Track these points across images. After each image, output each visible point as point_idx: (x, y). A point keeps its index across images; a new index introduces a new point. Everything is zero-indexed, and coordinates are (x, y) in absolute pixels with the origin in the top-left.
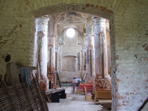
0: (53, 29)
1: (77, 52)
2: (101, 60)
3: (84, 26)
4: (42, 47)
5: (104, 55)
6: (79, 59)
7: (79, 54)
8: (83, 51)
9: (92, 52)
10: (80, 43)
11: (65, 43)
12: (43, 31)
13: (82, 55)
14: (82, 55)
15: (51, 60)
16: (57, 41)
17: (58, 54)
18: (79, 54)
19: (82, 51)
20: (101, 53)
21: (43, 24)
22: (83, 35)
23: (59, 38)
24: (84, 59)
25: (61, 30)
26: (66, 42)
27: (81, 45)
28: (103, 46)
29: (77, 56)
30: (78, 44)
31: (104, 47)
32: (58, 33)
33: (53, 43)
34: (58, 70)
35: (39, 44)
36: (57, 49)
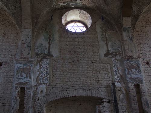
1: (105, 83)
7: (112, 89)
8: (129, 76)
10: (111, 50)
11: (58, 54)
13: (127, 91)
14: (127, 91)
17: (30, 93)
18: (112, 89)
19: (123, 79)
22: (120, 26)
24: (137, 106)
26: (60, 51)
27: (118, 58)
29: (106, 99)
30: (106, 55)
36: (29, 75)
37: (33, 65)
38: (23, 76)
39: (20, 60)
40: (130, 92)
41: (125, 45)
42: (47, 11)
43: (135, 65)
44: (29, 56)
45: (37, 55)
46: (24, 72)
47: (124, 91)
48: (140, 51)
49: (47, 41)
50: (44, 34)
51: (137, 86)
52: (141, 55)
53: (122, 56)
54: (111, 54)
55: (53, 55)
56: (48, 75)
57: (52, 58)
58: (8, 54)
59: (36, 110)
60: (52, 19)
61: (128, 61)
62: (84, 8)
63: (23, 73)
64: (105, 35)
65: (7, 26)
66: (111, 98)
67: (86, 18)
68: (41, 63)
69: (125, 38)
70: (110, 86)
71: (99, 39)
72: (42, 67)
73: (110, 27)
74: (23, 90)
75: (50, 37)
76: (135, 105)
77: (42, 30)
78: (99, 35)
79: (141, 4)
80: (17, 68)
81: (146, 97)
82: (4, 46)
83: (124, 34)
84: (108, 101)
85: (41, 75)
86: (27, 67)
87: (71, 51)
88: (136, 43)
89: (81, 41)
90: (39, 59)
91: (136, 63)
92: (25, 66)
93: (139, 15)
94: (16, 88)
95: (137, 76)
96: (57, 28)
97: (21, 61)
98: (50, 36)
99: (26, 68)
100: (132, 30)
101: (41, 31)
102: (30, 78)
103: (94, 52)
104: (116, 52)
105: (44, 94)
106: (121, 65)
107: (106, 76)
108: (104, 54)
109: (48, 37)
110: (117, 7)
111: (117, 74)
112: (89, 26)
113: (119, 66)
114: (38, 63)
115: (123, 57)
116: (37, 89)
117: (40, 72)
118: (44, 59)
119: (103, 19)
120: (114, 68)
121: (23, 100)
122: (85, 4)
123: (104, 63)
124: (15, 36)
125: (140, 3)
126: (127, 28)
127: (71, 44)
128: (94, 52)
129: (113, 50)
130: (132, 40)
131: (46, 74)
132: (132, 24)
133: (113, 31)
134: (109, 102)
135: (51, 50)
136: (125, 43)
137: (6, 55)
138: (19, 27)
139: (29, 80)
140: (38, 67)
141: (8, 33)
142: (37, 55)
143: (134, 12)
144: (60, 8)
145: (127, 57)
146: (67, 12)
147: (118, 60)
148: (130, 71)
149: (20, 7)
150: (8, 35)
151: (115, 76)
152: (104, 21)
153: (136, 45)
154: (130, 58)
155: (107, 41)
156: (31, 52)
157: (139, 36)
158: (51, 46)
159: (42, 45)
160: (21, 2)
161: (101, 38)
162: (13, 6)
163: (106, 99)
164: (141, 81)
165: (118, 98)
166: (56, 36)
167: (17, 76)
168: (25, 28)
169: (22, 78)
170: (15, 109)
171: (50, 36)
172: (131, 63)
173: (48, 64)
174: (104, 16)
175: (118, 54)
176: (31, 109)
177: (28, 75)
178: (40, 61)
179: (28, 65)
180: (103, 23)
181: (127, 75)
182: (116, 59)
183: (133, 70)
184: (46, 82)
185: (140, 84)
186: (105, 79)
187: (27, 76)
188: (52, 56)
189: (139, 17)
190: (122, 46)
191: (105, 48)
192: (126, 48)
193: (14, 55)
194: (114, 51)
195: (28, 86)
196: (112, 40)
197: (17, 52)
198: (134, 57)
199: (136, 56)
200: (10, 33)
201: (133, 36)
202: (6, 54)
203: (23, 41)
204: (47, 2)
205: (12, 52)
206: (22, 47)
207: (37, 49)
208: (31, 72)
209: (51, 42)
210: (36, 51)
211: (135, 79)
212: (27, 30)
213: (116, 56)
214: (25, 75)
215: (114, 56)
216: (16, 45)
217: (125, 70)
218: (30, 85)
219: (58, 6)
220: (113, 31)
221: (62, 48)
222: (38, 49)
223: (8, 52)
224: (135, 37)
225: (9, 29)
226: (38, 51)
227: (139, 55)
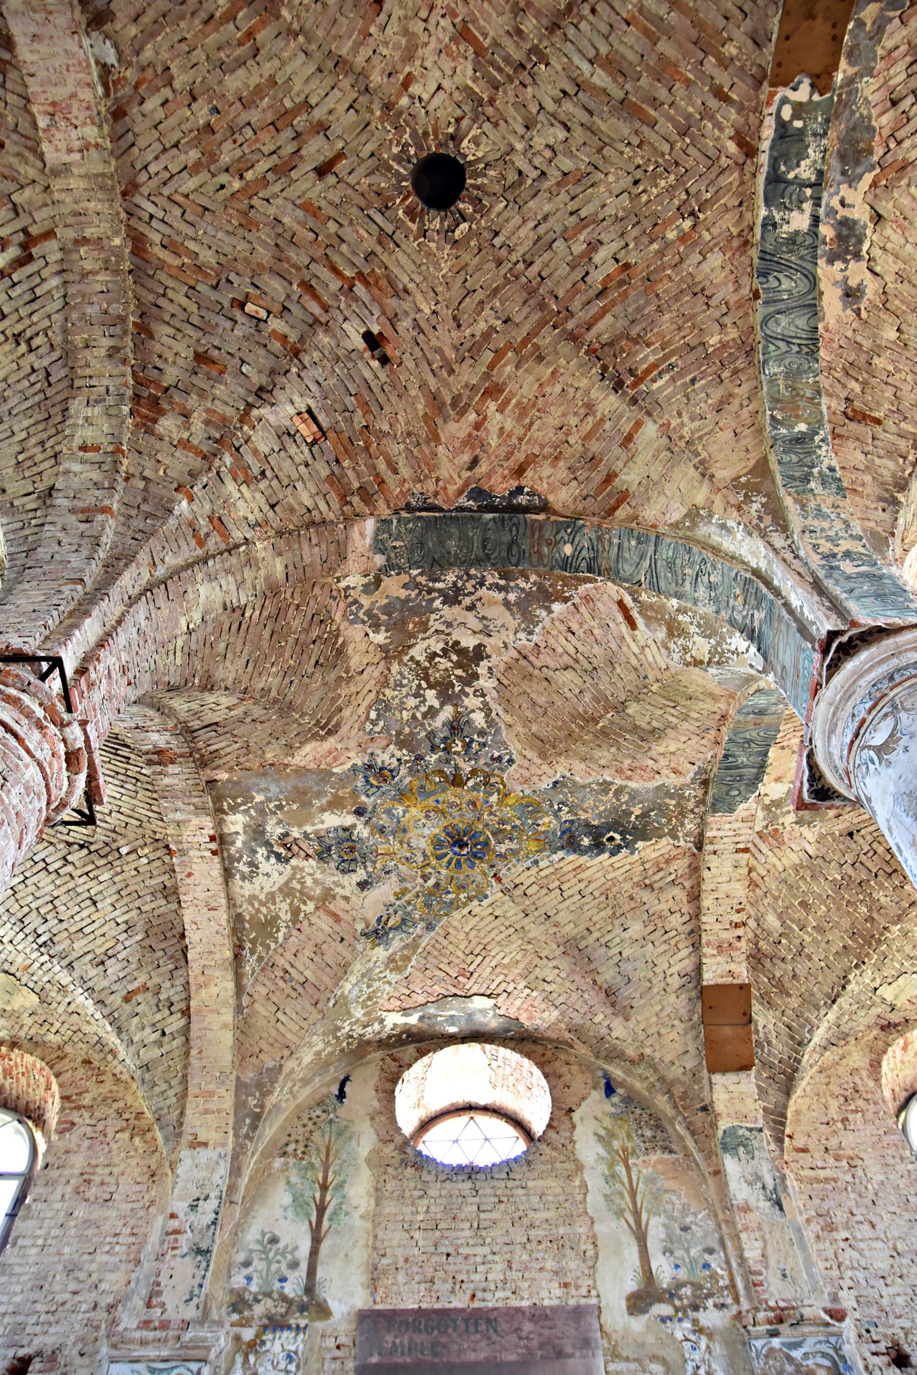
3: (695, 937)
16: (202, 1252)
27: (711, 1317)
32: (239, 1105)
39: (138, 1335)
41: (743, 1236)
42: (318, 1054)
44: (190, 1312)
48: (835, 1273)
49: (308, 1215)
50: (294, 1179)
52: (847, 1301)
53: (734, 1309)
54: (670, 1295)
57: (320, 1325)
58: (78, 1298)
60: (341, 1095)
61: (776, 1342)
62: (511, 1039)
64: (626, 1180)
65: (110, 1135)
67: (521, 1088)
68: (252, 1358)
69: (739, 1191)
71: (595, 1200)
73: (648, 1133)
75: (323, 1197)
77: (284, 1154)
78: (594, 1179)
79: (794, 1002)
82: (67, 1250)
87: (432, 1281)
88: (808, 1221)
89: (495, 1215)
90: (248, 1334)
91: (824, 1355)
93: (799, 1062)
97: (143, 1343)
98: (324, 1188)
100: (773, 1146)
101: (278, 1163)
103: (566, 1285)
104: (692, 1284)
109: (308, 1193)
110: (676, 1022)
112: (538, 1127)
114: (239, 1359)
115: (739, 1316)
118: (274, 1331)
119: (609, 1090)
122: (512, 1013)
123: (627, 1359)
124: (138, 1188)
125: (789, 995)
126: (740, 1132)
127: (438, 1234)
128: (566, 1285)
129: (677, 1266)
130: (779, 1204)
132: (765, 1109)
133: (671, 1152)
135: (319, 1274)
136: (741, 1220)
137: (63, 1304)
138: (167, 1139)
141: (107, 1171)
142: (239, 1303)
143: (769, 1043)
144: (389, 1037)
145: (761, 1315)
146: (426, 1060)
147: (710, 1336)
149: (186, 1030)
150: (102, 1184)
152: (615, 1099)
153: (809, 1234)
154: (781, 1321)
155: (637, 1214)
156: (206, 1283)
157: (818, 1181)
158: (325, 1247)
159: (274, 1240)
160: (188, 1008)
162: (148, 1030)
168: (197, 1144)
171: (324, 1188)
172: (797, 1354)
174: (617, 1072)
175: (710, 1295)
180: (613, 1110)
182: (699, 1330)
188: (324, 1311)
189: (796, 1070)
190: (729, 1244)
192: (752, 1253)
193: (111, 1308)
194: (682, 1274)
196: (668, 1207)
197: (133, 1285)
198: (807, 1312)
199: (815, 1309)
200: (116, 1171)
201: (783, 1178)
202: (67, 1296)
203: (173, 1216)
204: (319, 1006)
205: (103, 1286)
206: (160, 1257)
209: (326, 1224)
210: (238, 1281)
212: (204, 1155)
213: (696, 1308)
215: (684, 1309)
216: (132, 1239)
219: (377, 1027)
220: (666, 1156)
221: (385, 1261)
222: (251, 1269)
223: (81, 1286)
224: (791, 1182)
225: (114, 1152)
226: (249, 1279)
227: (835, 1298)
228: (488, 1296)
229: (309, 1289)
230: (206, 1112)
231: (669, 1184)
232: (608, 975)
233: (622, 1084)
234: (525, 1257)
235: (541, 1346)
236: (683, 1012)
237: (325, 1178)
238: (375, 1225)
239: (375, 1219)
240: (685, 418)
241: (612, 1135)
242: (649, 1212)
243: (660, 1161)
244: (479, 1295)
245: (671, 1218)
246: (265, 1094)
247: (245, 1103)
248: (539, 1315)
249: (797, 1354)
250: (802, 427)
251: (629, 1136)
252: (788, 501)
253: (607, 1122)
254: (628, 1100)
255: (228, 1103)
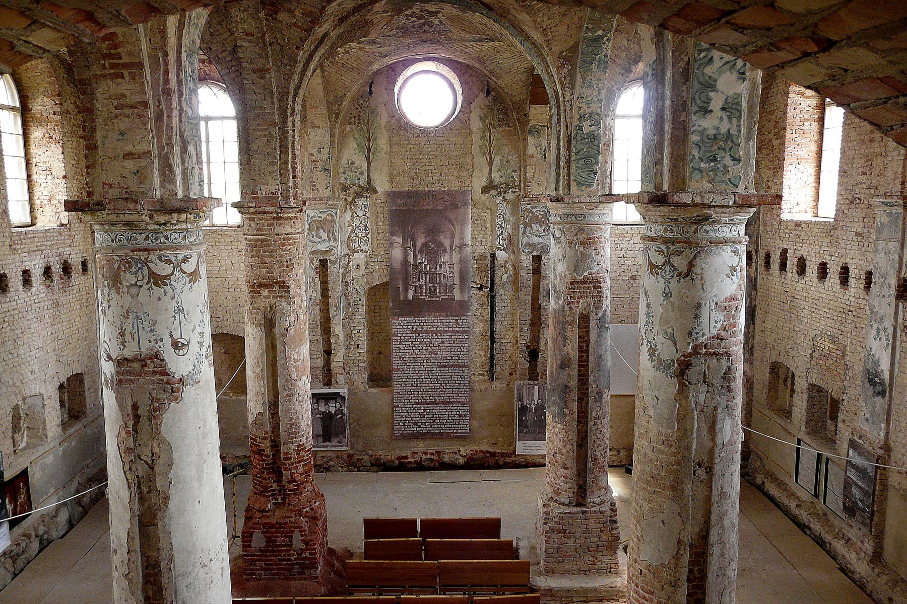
0: (283, 149)
1: (479, 251)
2: (685, 586)
4: (166, 500)
5: (716, 550)
6: (492, 298)
8: (525, 240)
9: (593, 337)
12: (168, 352)
15: (282, 395)
17: (335, 270)
19: (511, 243)
20: (690, 533)
21: (157, 280)
22: (524, 119)
23: (337, 143)
25: (356, 86)
27: (510, 196)
28: (710, 470)
30: (485, 190)
31: (717, 484)
33: (290, 266)
34: (341, 379)
35: (141, 469)
37: (338, 212)
38: (321, 238)
40: (521, 272)
43: (540, 217)
45: (344, 188)
46: (322, 228)
47: (511, 268)
49: (364, 153)
51: (537, 260)
55: (378, 188)
56: (368, 233)
59: (351, 301)
60: (371, 92)
61: (529, 207)
63: (321, 231)
66: (485, 281)
69: (531, 150)
70: (486, 257)
71: (475, 148)
72: (355, 215)
74: (323, 263)
76: (526, 297)
78: (476, 138)
80: (308, 221)
81: (548, 282)
83: (530, 140)
84: (479, 286)
85: (356, 234)
86: (328, 218)
90: (350, 199)
92: (323, 216)
94: (311, 261)
95: (540, 240)
96: (383, 119)
98: (369, 140)
99: (325, 219)
101: (348, 128)
102: (335, 239)
103: (461, 182)
105: (362, 271)
106: (512, 214)
107: (480, 237)
108: (482, 189)
109: (363, 143)
111: (502, 232)
113: (508, 215)
116: (349, 262)
117: (353, 227)
119: (488, 93)
120: (498, 220)
121: (327, 282)
128: (461, 182)
131: (364, 231)
134: (480, 289)
139: (334, 244)
140: (348, 216)
142: (344, 188)
148: (529, 229)
151: (498, 237)
152: (490, 98)
155: (490, 154)
159: (353, 163)
161: (480, 146)
163: (475, 282)
164: (546, 250)
165: (497, 281)
166: (383, 142)
167: (310, 237)
168: (314, 127)
169: (320, 240)
170: (315, 301)
171: (369, 140)
172: (534, 211)
173: (367, 210)
175: (510, 188)
176: (342, 300)
177: (331, 235)
178: (352, 202)
179: (328, 213)
181: (521, 237)
183: (535, 227)
184: (365, 248)
185: (543, 257)
186: (477, 243)
187: (328, 236)
188: (375, 192)
191: (486, 171)
194: (503, 180)
195: (333, 259)
196: (503, 152)
206: (311, 171)
207: (344, 173)
208: (337, 228)
210: (342, 180)
211: (534, 246)
212: (319, 131)
213: (505, 193)
214: (324, 236)
217: (519, 227)
218: (336, 255)
220: (507, 128)
222: (346, 175)
228: (433, 185)
229: (369, 183)
230: (316, 114)
231: (505, 142)
232: (491, 67)
233: (494, 90)
234: (447, 171)
235: (450, 204)
236: (523, 80)
237: (369, 136)
238: (391, 156)
239: (390, 154)
240: (545, 19)
241: (486, 117)
242: (495, 154)
243: (503, 131)
244: (430, 185)
245: (503, 157)
246: (339, 105)
247: (332, 109)
248: (451, 194)
249: (534, 211)
250: (600, 32)
251: (493, 118)
252: (579, 76)
253: (485, 111)
254: (495, 99)
255: (325, 112)
